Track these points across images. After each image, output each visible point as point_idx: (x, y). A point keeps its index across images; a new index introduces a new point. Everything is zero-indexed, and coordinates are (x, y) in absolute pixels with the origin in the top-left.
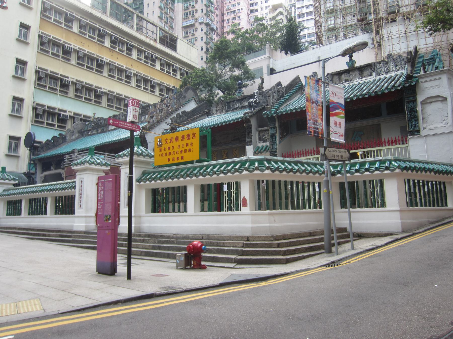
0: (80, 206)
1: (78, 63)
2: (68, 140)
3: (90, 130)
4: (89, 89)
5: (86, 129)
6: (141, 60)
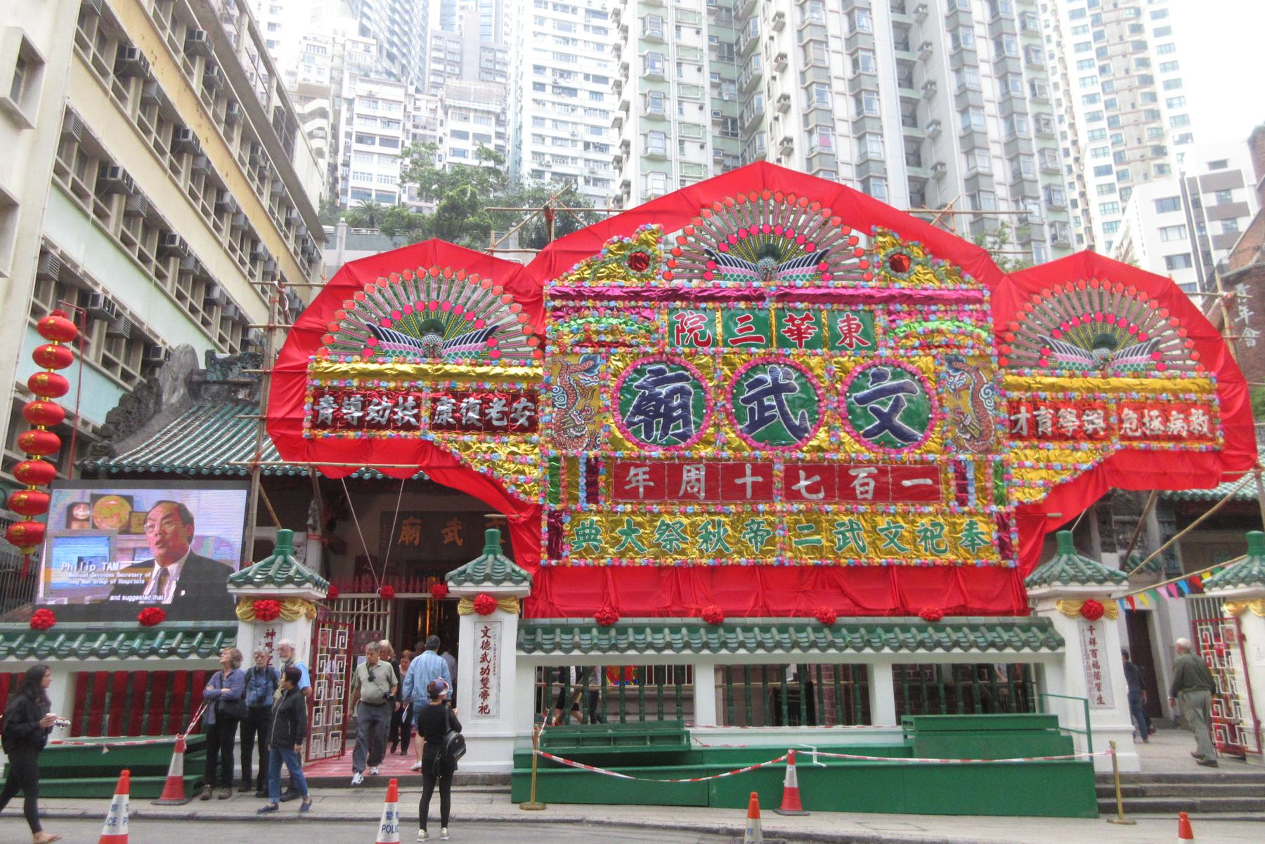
0: (1100, 699)
1: (140, 123)
2: (164, 407)
3: (244, 385)
4: (154, 225)
5: (212, 377)
6: (243, 164)
